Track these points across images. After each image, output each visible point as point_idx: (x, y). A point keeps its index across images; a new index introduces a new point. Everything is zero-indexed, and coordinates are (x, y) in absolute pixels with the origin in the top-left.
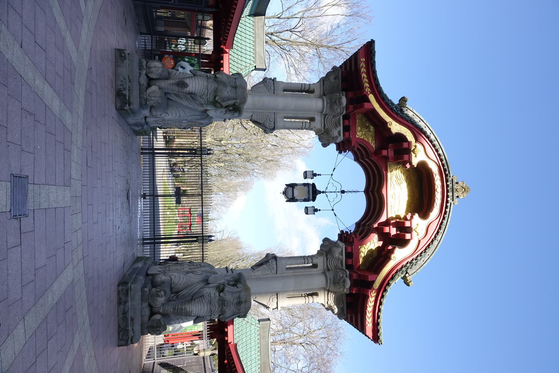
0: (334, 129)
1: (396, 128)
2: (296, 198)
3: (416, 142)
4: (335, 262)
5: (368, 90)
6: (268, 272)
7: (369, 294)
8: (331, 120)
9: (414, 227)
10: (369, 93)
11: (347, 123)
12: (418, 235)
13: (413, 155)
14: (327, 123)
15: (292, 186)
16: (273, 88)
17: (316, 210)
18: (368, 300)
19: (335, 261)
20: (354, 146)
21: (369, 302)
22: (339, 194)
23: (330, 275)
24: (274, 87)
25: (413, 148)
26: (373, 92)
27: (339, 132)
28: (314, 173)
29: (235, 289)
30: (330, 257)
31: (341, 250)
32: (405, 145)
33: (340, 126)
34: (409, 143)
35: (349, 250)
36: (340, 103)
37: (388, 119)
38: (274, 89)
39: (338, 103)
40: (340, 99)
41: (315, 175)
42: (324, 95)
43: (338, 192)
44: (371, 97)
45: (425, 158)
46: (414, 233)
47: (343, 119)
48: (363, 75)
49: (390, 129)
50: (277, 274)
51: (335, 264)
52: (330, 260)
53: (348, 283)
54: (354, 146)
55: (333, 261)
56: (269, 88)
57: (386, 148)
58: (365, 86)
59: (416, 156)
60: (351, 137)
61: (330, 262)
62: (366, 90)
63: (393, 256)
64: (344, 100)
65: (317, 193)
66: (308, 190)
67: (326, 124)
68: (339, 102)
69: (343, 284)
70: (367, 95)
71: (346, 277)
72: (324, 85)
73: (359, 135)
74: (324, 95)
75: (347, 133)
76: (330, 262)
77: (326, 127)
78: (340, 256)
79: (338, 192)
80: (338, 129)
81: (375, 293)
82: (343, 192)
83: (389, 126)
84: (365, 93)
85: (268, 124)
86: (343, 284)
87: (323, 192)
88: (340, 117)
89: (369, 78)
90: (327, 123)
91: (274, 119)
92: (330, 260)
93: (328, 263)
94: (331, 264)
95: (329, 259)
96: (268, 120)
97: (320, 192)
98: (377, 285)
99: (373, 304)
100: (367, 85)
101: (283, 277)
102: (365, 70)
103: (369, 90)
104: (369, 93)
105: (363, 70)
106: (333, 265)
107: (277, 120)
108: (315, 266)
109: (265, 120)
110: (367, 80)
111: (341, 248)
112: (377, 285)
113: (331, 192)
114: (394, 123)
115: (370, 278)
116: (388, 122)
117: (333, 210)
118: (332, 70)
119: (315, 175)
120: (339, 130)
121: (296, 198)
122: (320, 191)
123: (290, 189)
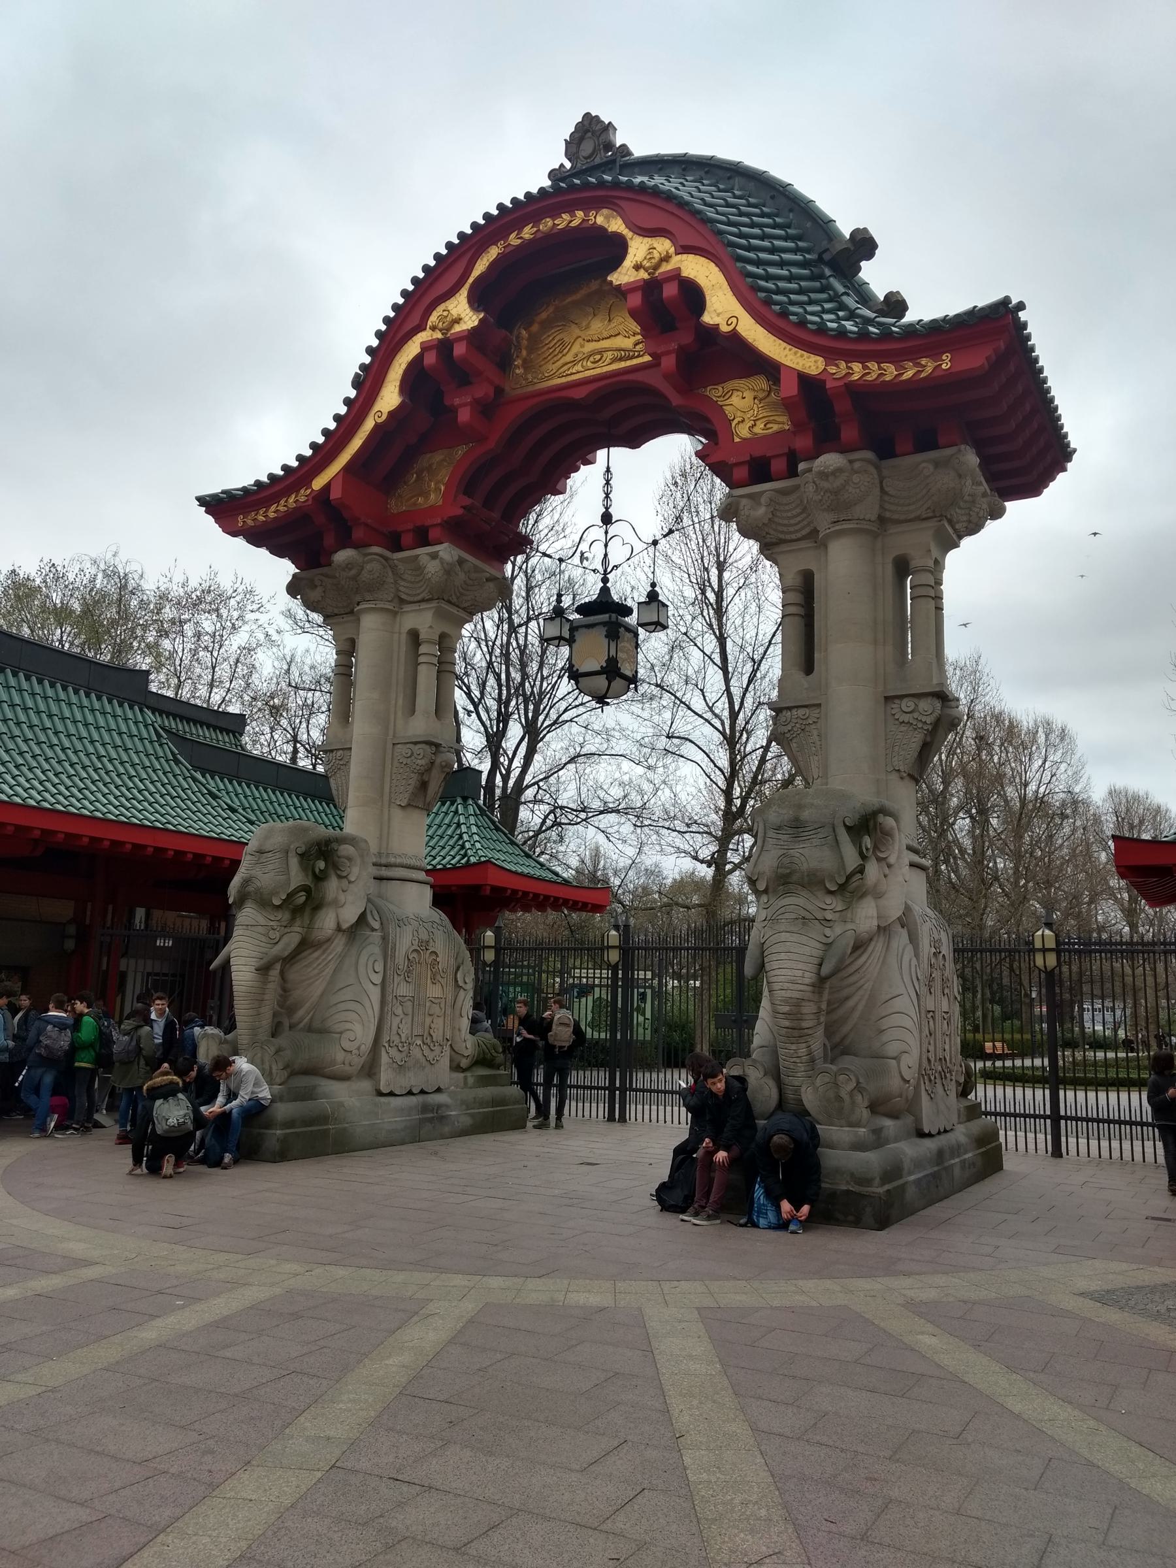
2: (604, 665)
3: (425, 329)
4: (789, 514)
5: (303, 495)
6: (815, 733)
7: (841, 383)
8: (412, 583)
9: (643, 275)
10: (309, 491)
11: (407, 539)
12: (666, 258)
13: (457, 328)
14: (419, 594)
17: (653, 596)
18: (861, 382)
19: (785, 515)
20: (462, 507)
21: (869, 378)
22: (613, 530)
25: (438, 335)
27: (434, 556)
30: (772, 532)
31: (744, 501)
32: (430, 359)
34: (425, 347)
37: (369, 425)
39: (353, 572)
42: (352, 612)
43: (606, 533)
44: (318, 483)
45: (464, 292)
47: (400, 549)
49: (391, 413)
50: (819, 705)
51: (794, 512)
52: (782, 532)
53: (830, 460)
54: (462, 507)
55: (786, 522)
57: (453, 411)
59: (458, 321)
60: (439, 521)
61: (791, 529)
63: (725, 328)
64: (342, 556)
66: (584, 630)
67: (419, 598)
68: (350, 569)
69: (831, 478)
70: (313, 495)
72: (336, 615)
73: (434, 499)
74: (352, 612)
75: (433, 534)
76: (791, 529)
77: (425, 595)
78: (763, 500)
79: (606, 533)
80: (424, 560)
81: (837, 366)
82: (607, 519)
83: (384, 417)
85: (419, 762)
86: (831, 478)
87: (605, 580)
88: (397, 559)
90: (419, 594)
91: (408, 746)
92: (782, 532)
93: (793, 537)
94: (797, 528)
95: (782, 536)
96: (409, 761)
97: (605, 591)
98: (811, 364)
99: (873, 365)
103: (302, 491)
104: (309, 491)
106: (799, 519)
110: (282, 502)
111: (738, 504)
112: (811, 364)
113: (606, 555)
117: (655, 543)
118: (299, 597)
120: (427, 558)
122: (601, 589)
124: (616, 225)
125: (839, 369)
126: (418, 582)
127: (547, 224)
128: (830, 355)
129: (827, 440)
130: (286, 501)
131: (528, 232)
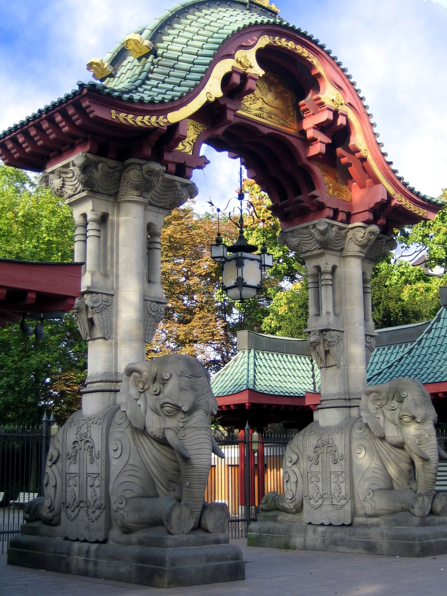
0: (177, 192)
2: (260, 284)
3: (234, 58)
14: (161, 203)
16: (105, 297)
24: (102, 293)
26: (165, 112)
28: (216, 243)
32: (236, 79)
33: (173, 181)
34: (234, 71)
35: (331, 213)
36: (157, 174)
38: (106, 294)
43: (241, 205)
48: (140, 124)
56: (104, 303)
58: (156, 125)
62: (162, 124)
65: (245, 245)
67: (161, 205)
70: (169, 124)
71: (365, 228)
79: (241, 205)
80: (179, 187)
83: (212, 99)
84: (165, 128)
89: (144, 113)
95: (333, 248)
100: (154, 119)
102: (131, 116)
103: (161, 118)
106: (338, 242)
107: (155, 297)
109: (154, 320)
110: (147, 117)
112: (392, 191)
114: (207, 88)
116: (206, 100)
121: (260, 284)
126: (161, 195)
130: (150, 119)
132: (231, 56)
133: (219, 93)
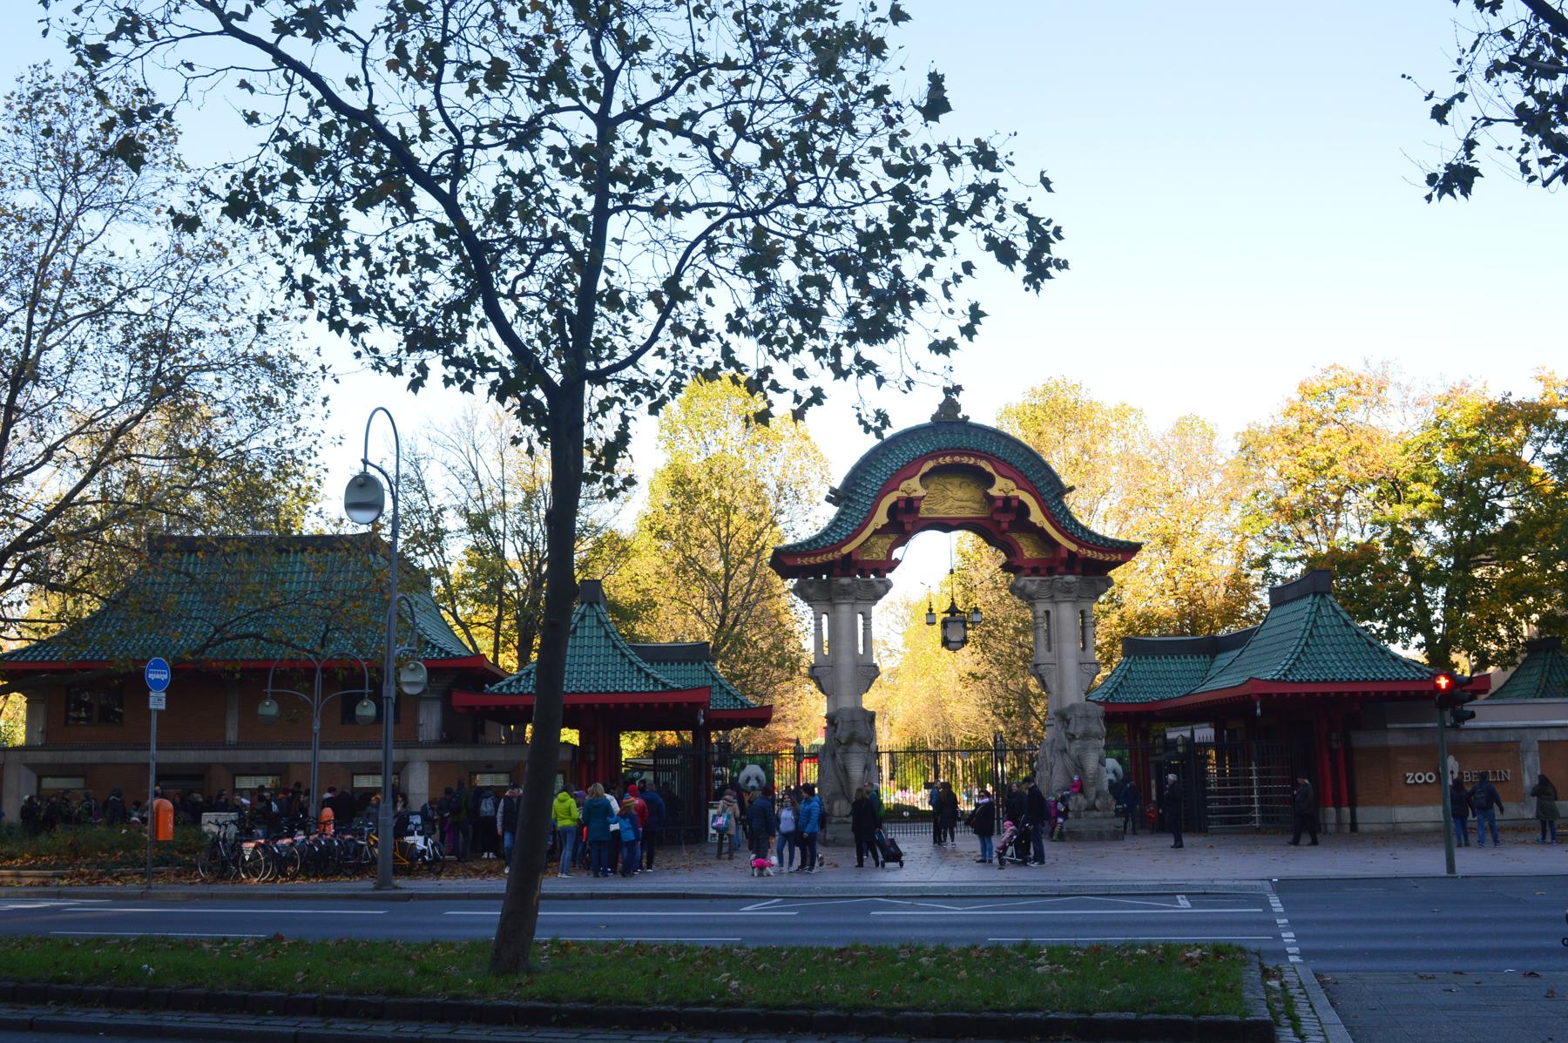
1: (881, 518)
5: (837, 555)
9: (1002, 494)
15: (946, 643)
23: (1059, 597)
25: (905, 495)
26: (839, 549)
29: (1073, 722)
32: (902, 505)
34: (899, 499)
36: (849, 585)
40: (842, 585)
41: (931, 610)
46: (1011, 494)
74: (830, 600)
89: (822, 554)
97: (953, 604)
98: (1073, 547)
101: (1060, 658)
105: (812, 560)
108: (1047, 613)
112: (1073, 547)
115: (1065, 555)
119: (931, 610)
123: (951, 645)
124: (989, 469)
125: (1083, 551)
127: (957, 459)
128: (1080, 546)
129: (1071, 571)
131: (948, 459)
132: (897, 489)
133: (885, 520)
